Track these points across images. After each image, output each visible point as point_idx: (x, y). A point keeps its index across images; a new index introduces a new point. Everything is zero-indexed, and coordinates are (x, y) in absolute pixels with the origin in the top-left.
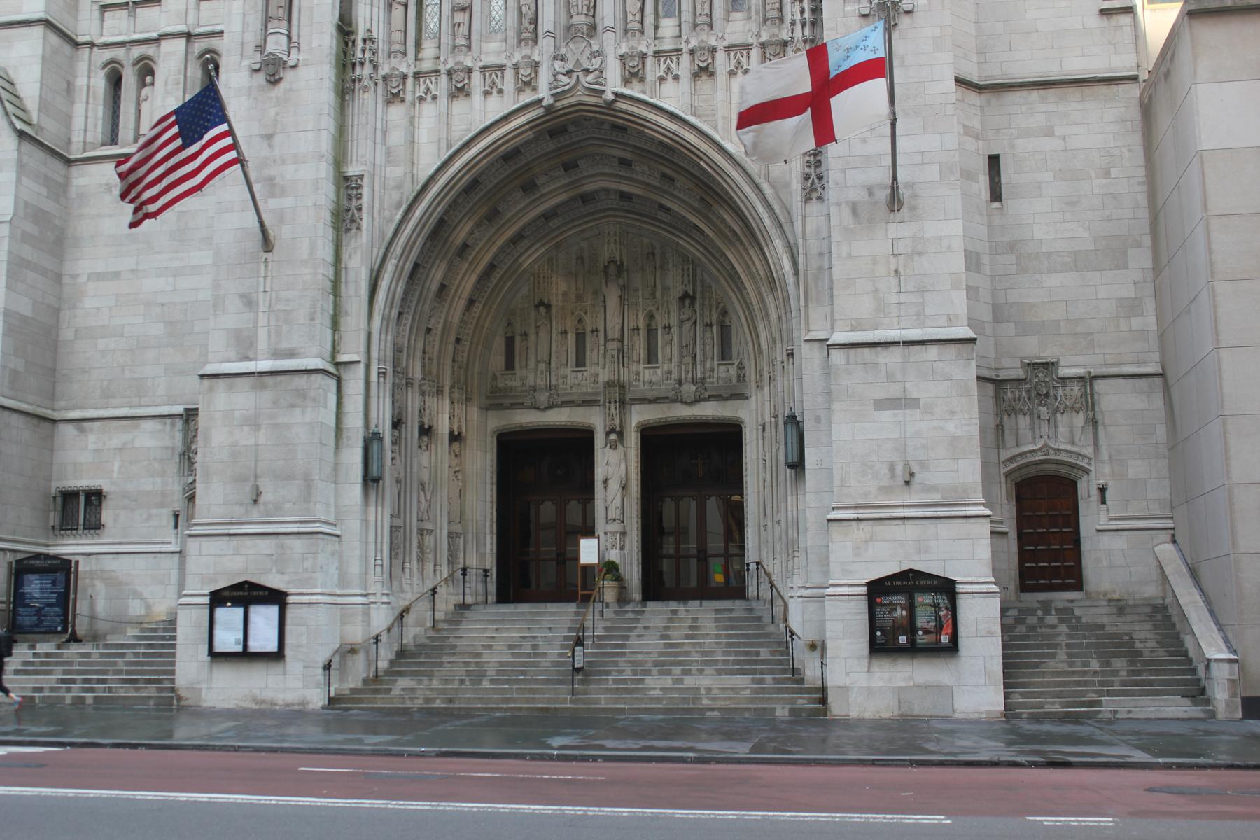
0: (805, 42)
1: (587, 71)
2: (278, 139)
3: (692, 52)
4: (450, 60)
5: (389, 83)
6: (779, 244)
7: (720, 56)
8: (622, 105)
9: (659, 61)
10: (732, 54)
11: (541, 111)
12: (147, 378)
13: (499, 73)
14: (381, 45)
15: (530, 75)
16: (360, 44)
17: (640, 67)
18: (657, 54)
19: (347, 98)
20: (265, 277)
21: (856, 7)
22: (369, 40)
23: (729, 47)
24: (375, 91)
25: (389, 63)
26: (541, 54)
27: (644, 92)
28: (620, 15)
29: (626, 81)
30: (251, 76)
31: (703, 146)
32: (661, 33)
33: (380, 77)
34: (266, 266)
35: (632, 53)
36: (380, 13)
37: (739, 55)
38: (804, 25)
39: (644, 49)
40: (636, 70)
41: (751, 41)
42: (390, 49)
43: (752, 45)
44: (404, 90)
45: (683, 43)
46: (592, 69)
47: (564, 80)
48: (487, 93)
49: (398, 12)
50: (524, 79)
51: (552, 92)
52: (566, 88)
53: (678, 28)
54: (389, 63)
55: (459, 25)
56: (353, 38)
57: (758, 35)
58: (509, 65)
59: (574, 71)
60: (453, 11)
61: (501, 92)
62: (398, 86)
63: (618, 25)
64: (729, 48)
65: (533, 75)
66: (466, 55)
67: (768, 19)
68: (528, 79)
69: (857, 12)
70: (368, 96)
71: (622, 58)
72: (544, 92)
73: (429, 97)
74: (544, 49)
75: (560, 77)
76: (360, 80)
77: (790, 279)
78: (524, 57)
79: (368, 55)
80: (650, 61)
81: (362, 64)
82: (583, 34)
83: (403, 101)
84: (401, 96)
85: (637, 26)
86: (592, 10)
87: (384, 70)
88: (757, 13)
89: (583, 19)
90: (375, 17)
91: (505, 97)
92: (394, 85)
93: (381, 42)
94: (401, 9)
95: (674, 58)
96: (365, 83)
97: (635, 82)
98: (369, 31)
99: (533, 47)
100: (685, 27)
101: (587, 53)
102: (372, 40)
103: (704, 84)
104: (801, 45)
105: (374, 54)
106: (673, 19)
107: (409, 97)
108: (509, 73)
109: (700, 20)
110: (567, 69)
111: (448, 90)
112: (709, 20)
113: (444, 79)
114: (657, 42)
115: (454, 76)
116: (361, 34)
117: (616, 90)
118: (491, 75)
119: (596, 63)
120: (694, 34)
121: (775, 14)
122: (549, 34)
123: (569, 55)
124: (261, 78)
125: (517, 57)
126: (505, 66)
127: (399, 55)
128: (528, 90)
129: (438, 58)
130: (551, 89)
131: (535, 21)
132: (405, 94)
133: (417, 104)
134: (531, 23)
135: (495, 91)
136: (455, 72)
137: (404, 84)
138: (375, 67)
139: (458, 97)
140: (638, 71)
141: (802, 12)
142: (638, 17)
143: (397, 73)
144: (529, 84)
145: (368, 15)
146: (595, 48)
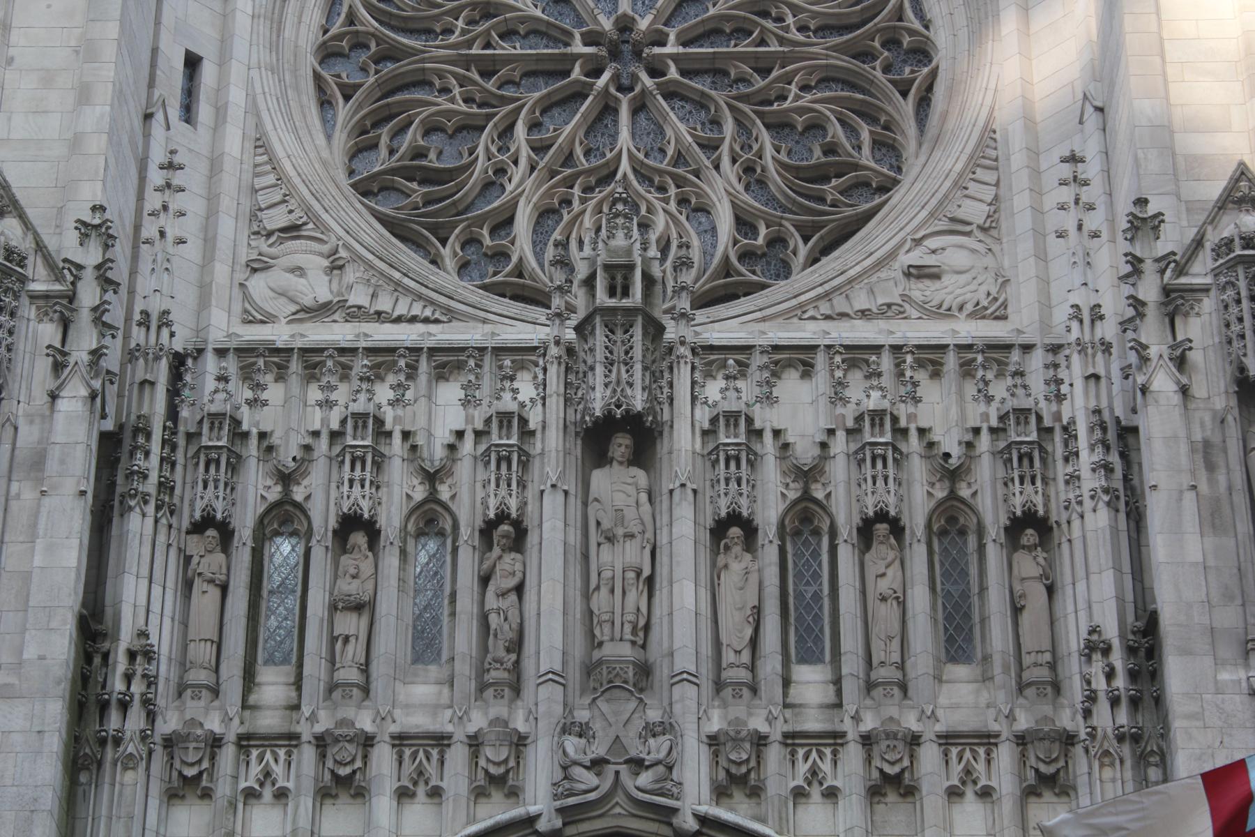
0: (1121, 738)
1: (638, 765)
3: (867, 740)
4: (322, 714)
5: (177, 753)
7: (929, 755)
9: (793, 753)
10: (954, 751)
13: (435, 753)
14: (163, 668)
15: (506, 761)
16: (121, 664)
17: (753, 763)
18: (792, 739)
19: (83, 778)
21: (1242, 674)
22: (142, 653)
23: (946, 737)
24: (148, 769)
25: (182, 710)
26: (534, 718)
27: (763, 820)
28: (707, 649)
29: (721, 793)
32: (795, 694)
33: (158, 739)
35: (738, 732)
36: (166, 600)
37: (968, 754)
38: (1115, 702)
39: (763, 728)
40: (744, 769)
41: (995, 727)
42: (181, 678)
43: (997, 736)
44: (211, 770)
45: (847, 720)
46: (649, 759)
47: (589, 779)
48: (404, 794)
49: (205, 600)
50: (493, 770)
51: (558, 804)
52: (592, 796)
53: (831, 688)
54: (182, 710)
55: (346, 639)
56: (106, 645)
57: (1011, 717)
58: (459, 735)
59: (607, 762)
60: (333, 608)
61: (436, 793)
62: (200, 762)
63: (704, 671)
64: (947, 739)
65: (512, 763)
66: (359, 707)
67: (1030, 684)
68: (502, 770)
69: (1244, 684)
70: (129, 776)
71: (714, 741)
73: (268, 793)
74: (542, 709)
75: (578, 772)
76: (117, 742)
78: (495, 722)
79: (137, 688)
80: (774, 754)
81: (124, 706)
82: (626, 682)
83: (207, 795)
84: (204, 783)
85: (744, 675)
86: (641, 634)
87: (169, 723)
88: (1006, 669)
89: (626, 650)
90: (156, 607)
91: (448, 806)
92: (192, 758)
93: (164, 660)
94: (215, 593)
95: (828, 751)
96: (130, 750)
97: (738, 795)
98: (143, 634)
99: (512, 701)
100: (851, 689)
101: (638, 725)
102: (149, 655)
103: (894, 812)
104: (1112, 745)
105: (149, 686)
106: (819, 667)
107: (223, 789)
108: (458, 756)
109: (881, 674)
110: (591, 756)
111: (316, 780)
112: (899, 675)
113: (308, 754)
114: (788, 713)
115: (331, 751)
116: (126, 638)
117: (703, 809)
118: (414, 756)
119: (657, 748)
120: (868, 702)
121: (1044, 674)
122: (557, 677)
123: (597, 726)
125: (478, 721)
126: (450, 737)
127: (204, 692)
128: (497, 796)
129: (296, 707)
130: (556, 797)
131: (517, 645)
132: (211, 779)
133: (240, 806)
134: (508, 650)
135: (421, 790)
136: (337, 740)
137: (213, 758)
138: (151, 717)
139: (336, 797)
140: (749, 771)
141: (1110, 675)
142: (746, 657)
143: (199, 732)
145: (142, 600)
146: (654, 715)
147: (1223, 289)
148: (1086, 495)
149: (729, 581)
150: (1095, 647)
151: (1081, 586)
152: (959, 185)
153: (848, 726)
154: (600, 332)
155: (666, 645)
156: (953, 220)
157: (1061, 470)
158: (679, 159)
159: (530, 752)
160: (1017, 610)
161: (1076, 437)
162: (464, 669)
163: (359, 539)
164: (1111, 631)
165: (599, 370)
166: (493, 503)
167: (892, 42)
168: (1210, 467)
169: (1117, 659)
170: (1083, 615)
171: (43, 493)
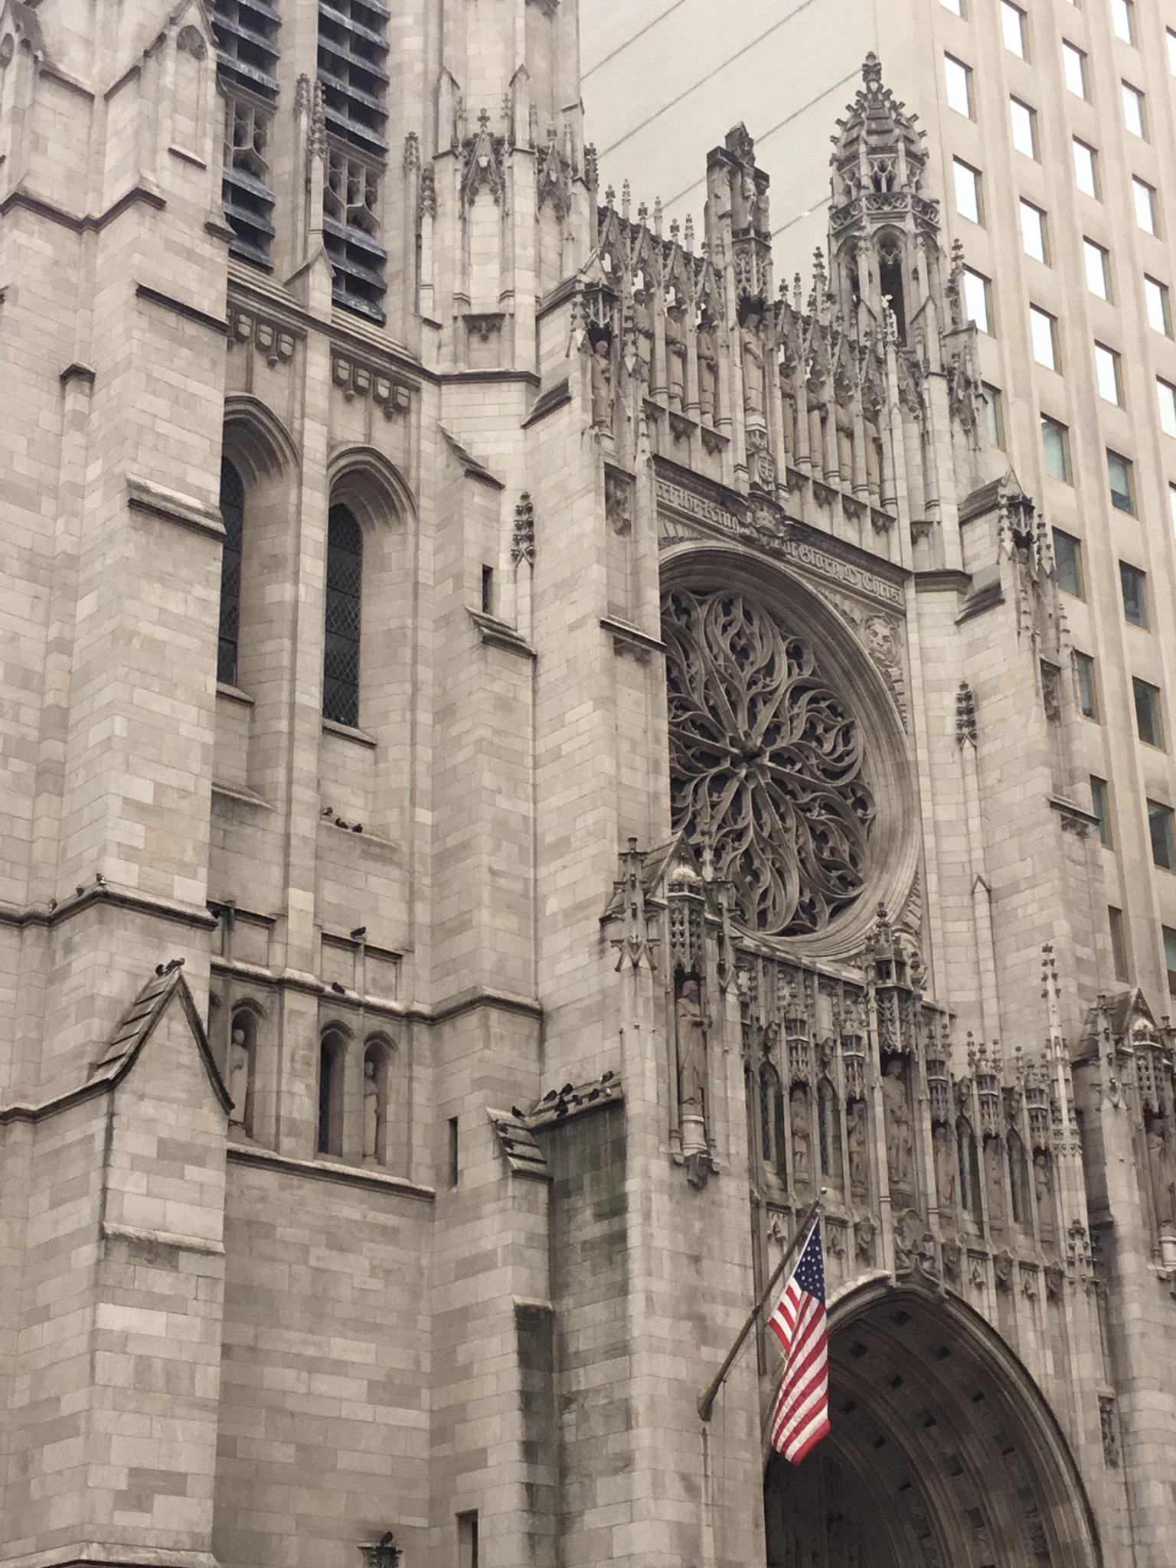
1: (923, 1256)
2: (706, 1264)
6: (1077, 1504)
8: (952, 1310)
11: (882, 1291)
12: (271, 1534)
20: (705, 1455)
30: (672, 1169)
31: (1014, 1375)
34: (705, 1440)
38: (1088, 1263)
47: (907, 1262)
60: (794, 1134)
72: (886, 1267)
77: (1088, 1549)
124: (681, 1177)
130: (897, 1269)
141: (1085, 1248)
144: (865, 1255)
147: (1139, 1058)
148: (1068, 1147)
149: (941, 1157)
150: (1076, 1231)
151: (1065, 1193)
152: (906, 904)
153: (988, 1249)
154: (895, 1000)
155: (921, 1188)
156: (906, 924)
157: (1053, 1127)
158: (770, 836)
159: (878, 1241)
160: (1039, 1199)
161: (1060, 1111)
162: (847, 1181)
163: (799, 1094)
164: (1085, 1223)
165: (898, 1023)
166: (858, 1090)
167: (854, 793)
168: (1136, 1153)
169: (1087, 1239)
170: (1065, 1210)
171: (726, 1052)
